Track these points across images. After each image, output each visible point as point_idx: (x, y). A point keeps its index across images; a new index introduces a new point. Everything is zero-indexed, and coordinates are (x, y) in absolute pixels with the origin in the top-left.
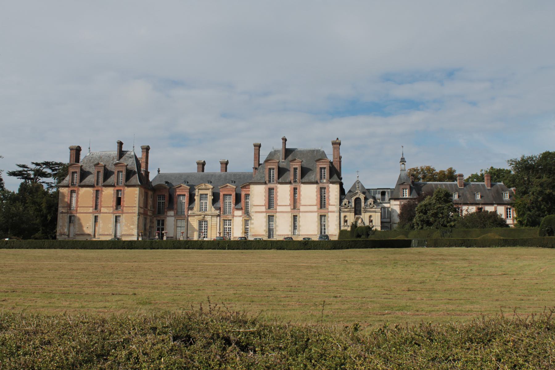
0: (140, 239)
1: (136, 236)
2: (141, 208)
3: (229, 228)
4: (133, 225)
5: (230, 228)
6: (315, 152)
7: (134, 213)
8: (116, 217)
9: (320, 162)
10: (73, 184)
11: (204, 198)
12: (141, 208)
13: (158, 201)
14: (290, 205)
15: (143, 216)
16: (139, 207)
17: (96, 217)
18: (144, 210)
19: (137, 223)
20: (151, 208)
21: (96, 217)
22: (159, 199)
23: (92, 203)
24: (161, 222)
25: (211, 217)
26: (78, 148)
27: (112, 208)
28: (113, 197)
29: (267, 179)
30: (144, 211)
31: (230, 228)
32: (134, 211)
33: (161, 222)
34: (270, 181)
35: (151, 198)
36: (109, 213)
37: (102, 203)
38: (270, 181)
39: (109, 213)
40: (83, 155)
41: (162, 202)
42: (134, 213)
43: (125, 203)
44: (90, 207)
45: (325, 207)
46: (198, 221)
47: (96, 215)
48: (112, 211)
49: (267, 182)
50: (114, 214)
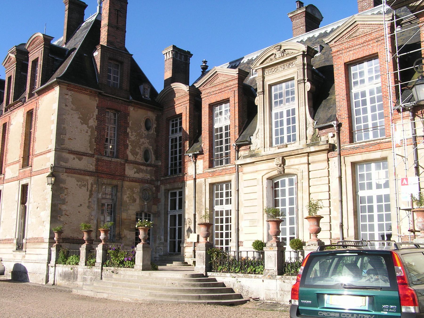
1: (47, 245)
2: (71, 152)
3: (379, 199)
5: (387, 198)
11: (284, 98)
12: (71, 152)
13: (171, 136)
15: (90, 180)
18: (98, 160)
20: (146, 159)
22: (173, 132)
24: (178, 198)
25: (304, 159)
28: (21, 132)
30: (97, 165)
31: (387, 198)
33: (178, 198)
35: (148, 128)
43: (36, 145)
46: (265, 181)
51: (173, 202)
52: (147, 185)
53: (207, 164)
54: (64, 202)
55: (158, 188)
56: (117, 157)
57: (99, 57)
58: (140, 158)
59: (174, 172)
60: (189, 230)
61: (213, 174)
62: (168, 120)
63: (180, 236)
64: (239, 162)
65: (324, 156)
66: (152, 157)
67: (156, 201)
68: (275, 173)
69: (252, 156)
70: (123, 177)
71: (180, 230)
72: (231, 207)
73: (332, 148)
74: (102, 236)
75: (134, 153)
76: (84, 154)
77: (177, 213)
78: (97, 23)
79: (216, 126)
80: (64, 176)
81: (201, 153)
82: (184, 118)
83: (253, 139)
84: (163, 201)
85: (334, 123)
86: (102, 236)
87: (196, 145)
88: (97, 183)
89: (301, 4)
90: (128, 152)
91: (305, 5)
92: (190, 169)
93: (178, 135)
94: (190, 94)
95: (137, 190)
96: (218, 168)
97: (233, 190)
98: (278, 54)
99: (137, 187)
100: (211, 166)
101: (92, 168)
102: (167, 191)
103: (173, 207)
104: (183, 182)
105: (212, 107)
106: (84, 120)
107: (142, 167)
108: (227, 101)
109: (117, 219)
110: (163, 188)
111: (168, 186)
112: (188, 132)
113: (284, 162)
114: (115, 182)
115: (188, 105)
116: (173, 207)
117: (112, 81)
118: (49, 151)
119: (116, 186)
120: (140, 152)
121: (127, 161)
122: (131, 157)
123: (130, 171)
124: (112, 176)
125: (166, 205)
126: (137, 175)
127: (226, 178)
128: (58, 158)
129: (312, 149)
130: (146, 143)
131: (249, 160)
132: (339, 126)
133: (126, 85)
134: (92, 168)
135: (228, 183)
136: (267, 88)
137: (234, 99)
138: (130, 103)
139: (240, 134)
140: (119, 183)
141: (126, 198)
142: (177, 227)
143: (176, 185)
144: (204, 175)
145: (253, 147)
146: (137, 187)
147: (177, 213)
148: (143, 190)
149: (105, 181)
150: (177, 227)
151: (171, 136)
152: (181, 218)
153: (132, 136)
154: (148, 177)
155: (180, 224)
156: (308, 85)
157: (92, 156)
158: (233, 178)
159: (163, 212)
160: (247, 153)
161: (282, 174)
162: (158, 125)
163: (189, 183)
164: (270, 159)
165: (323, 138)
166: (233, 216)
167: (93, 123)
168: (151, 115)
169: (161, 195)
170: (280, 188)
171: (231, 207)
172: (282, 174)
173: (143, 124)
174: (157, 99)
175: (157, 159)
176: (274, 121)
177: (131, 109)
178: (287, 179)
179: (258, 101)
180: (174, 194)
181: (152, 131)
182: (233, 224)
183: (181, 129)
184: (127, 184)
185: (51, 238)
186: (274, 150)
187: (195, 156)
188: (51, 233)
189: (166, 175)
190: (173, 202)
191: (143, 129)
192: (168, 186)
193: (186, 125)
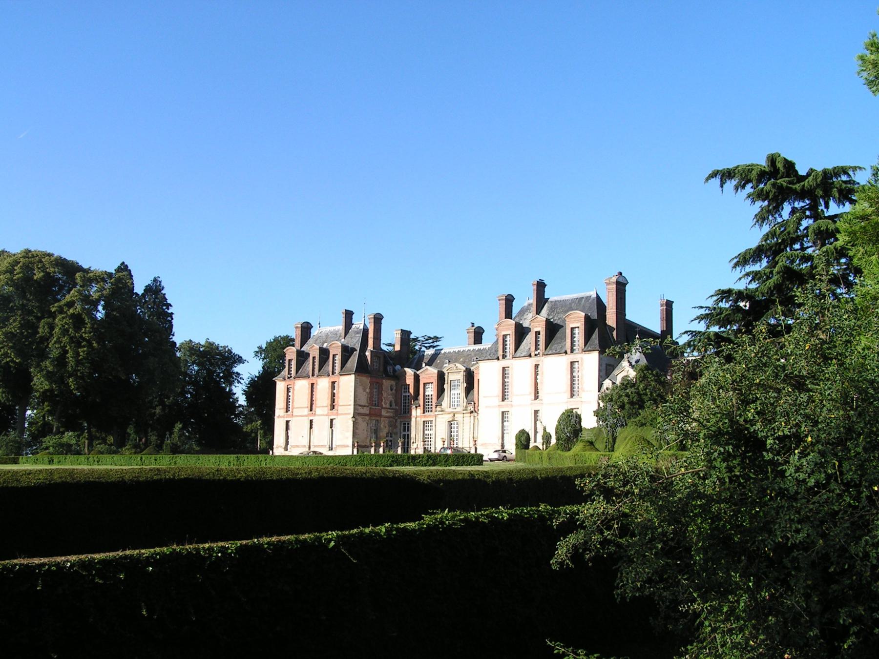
0: (355, 453)
1: (351, 448)
2: (360, 406)
4: (348, 431)
6: (584, 300)
7: (349, 414)
8: (332, 420)
9: (571, 318)
10: (289, 376)
11: (456, 387)
12: (360, 406)
14: (530, 394)
15: (367, 418)
16: (356, 404)
17: (311, 421)
19: (352, 429)
20: (391, 406)
21: (311, 421)
23: (307, 403)
24: (407, 426)
25: (462, 415)
26: (304, 325)
27: (326, 408)
29: (500, 353)
32: (349, 412)
33: (407, 426)
34: (504, 357)
35: (392, 390)
36: (324, 415)
37: (317, 402)
38: (504, 357)
39: (324, 415)
40: (314, 332)
41: (408, 396)
42: (349, 414)
44: (305, 408)
45: (578, 395)
46: (447, 423)
47: (311, 418)
48: (326, 413)
49: (501, 358)
50: (329, 416)
51: (404, 428)
52: (391, 419)
53: (422, 411)
54: (357, 429)
55: (396, 420)
56: (378, 406)
57: (370, 356)
58: (388, 406)
59: (405, 413)
60: (413, 443)
61: (425, 416)
62: (402, 385)
63: (408, 445)
64: (436, 413)
65: (469, 415)
66: (394, 404)
67: (396, 427)
68: (451, 419)
69: (442, 411)
70: (380, 416)
71: (408, 442)
72: (432, 432)
73: (472, 412)
74: (382, 444)
75: (386, 404)
76: (365, 406)
77: (406, 433)
78: (365, 331)
79: (427, 393)
80: (357, 417)
81: (419, 406)
82: (410, 387)
83: (443, 403)
84: (399, 427)
85: (473, 403)
86: (373, 444)
87: (417, 402)
88: (370, 419)
89: (473, 324)
90: (383, 403)
91: (476, 326)
92: (414, 412)
93: (407, 394)
94: (414, 375)
95: (387, 422)
96: (427, 414)
97: (433, 424)
98: (455, 368)
99: (387, 420)
100: (424, 413)
101: (368, 412)
102: (401, 422)
103: (404, 430)
104: (411, 419)
105: (425, 384)
106: (365, 391)
107: (389, 410)
108: (432, 383)
109: (378, 436)
110: (399, 420)
111: (402, 420)
112: (413, 394)
113: (454, 416)
114: (377, 418)
115: (413, 381)
116: (404, 430)
117: (375, 367)
118: (350, 405)
119: (378, 420)
120: (388, 402)
121: (382, 408)
122: (384, 406)
123: (384, 413)
124: (376, 415)
125: (400, 429)
126: (387, 414)
127: (431, 419)
128: (355, 409)
129: (465, 412)
130: (391, 398)
131: (441, 413)
132: (475, 404)
133: (382, 369)
134: (368, 412)
135: (431, 421)
136: (449, 382)
137: (435, 383)
138: (384, 378)
139: (438, 399)
140: (379, 419)
141: (382, 426)
142: (406, 440)
143: (406, 420)
144: (421, 417)
145: (442, 407)
146: (387, 420)
147: (406, 433)
148: (390, 422)
149: (373, 418)
150: (406, 440)
151: (403, 394)
152: (409, 437)
153: (385, 395)
154: (392, 415)
155: (408, 438)
156: (465, 384)
157: (368, 406)
158: (433, 419)
159: (399, 432)
160: (440, 409)
161: (453, 420)
162: (396, 387)
163: (413, 420)
164: (449, 413)
165: (469, 408)
166: (433, 436)
167: (368, 390)
168: (393, 383)
169: (398, 424)
170: (452, 426)
171: (432, 432)
172: (454, 420)
173: (389, 388)
174: (396, 374)
175: (396, 405)
176: (452, 396)
177: (384, 381)
178: (455, 422)
179: (446, 386)
180: (405, 424)
181: (394, 391)
182: (433, 440)
183: (409, 391)
184: (382, 419)
185: (353, 445)
186: (450, 410)
187: (416, 407)
188: (353, 442)
189: (401, 414)
190: (404, 428)
191: (390, 390)
192: (402, 420)
193: (412, 390)
